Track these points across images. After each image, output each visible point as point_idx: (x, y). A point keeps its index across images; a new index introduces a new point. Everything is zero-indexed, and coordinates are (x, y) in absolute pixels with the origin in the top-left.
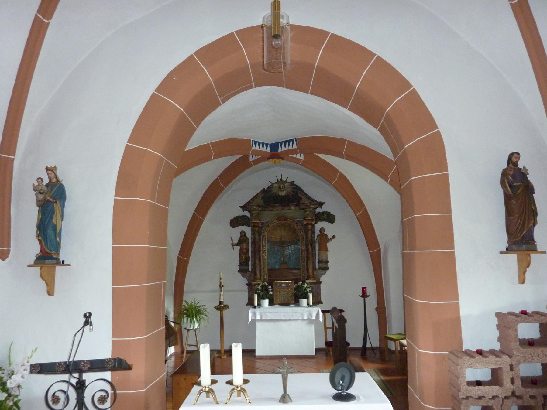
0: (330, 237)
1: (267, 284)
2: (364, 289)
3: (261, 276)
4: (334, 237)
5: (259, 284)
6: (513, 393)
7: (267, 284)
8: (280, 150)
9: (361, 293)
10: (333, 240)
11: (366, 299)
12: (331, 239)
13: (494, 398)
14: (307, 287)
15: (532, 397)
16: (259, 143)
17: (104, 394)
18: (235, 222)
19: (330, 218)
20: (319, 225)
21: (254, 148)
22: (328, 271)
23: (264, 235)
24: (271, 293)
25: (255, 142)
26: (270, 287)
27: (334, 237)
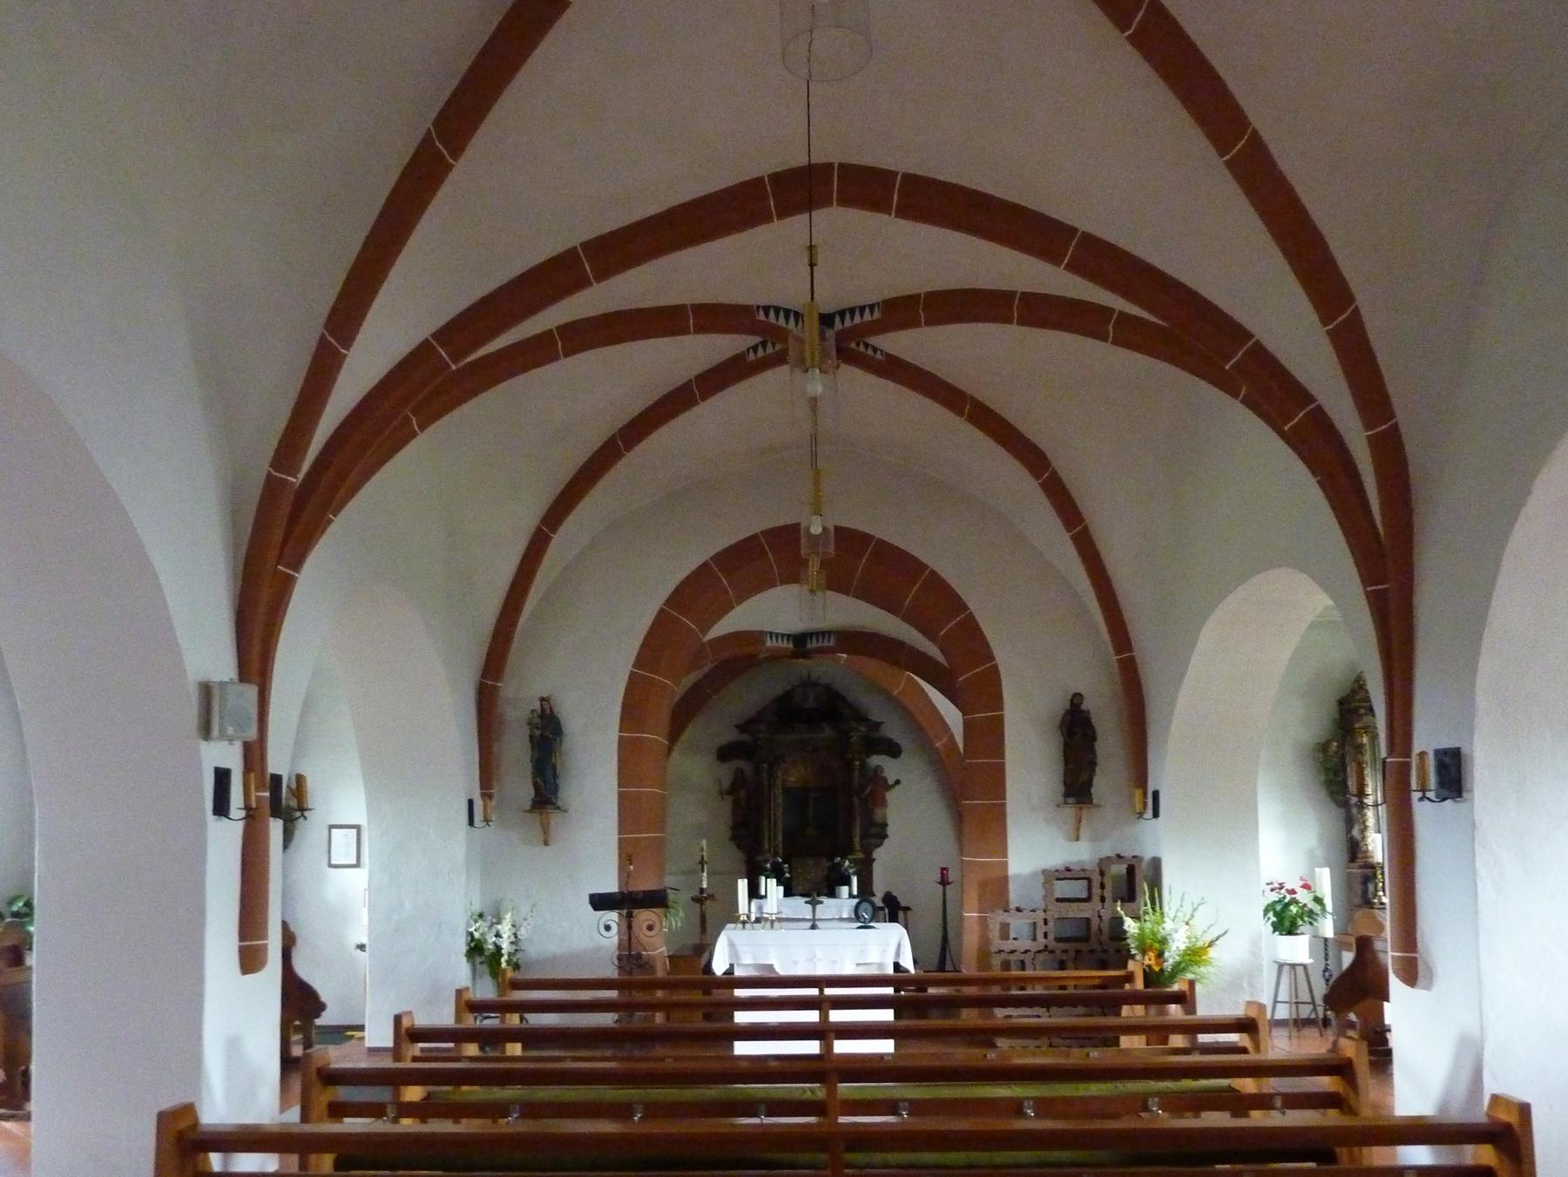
0: (891, 782)
1: (781, 860)
2: (944, 870)
3: (770, 849)
4: (898, 782)
5: (767, 861)
6: (1046, 946)
7: (781, 860)
8: (809, 646)
9: (938, 877)
10: (897, 787)
11: (948, 887)
12: (893, 786)
13: (1026, 952)
14: (848, 866)
15: (1065, 951)
16: (777, 634)
17: (651, 922)
18: (724, 754)
19: (894, 750)
20: (875, 760)
21: (769, 643)
22: (886, 841)
23: (778, 777)
24: (787, 875)
25: (771, 633)
26: (786, 866)
27: (898, 782)
